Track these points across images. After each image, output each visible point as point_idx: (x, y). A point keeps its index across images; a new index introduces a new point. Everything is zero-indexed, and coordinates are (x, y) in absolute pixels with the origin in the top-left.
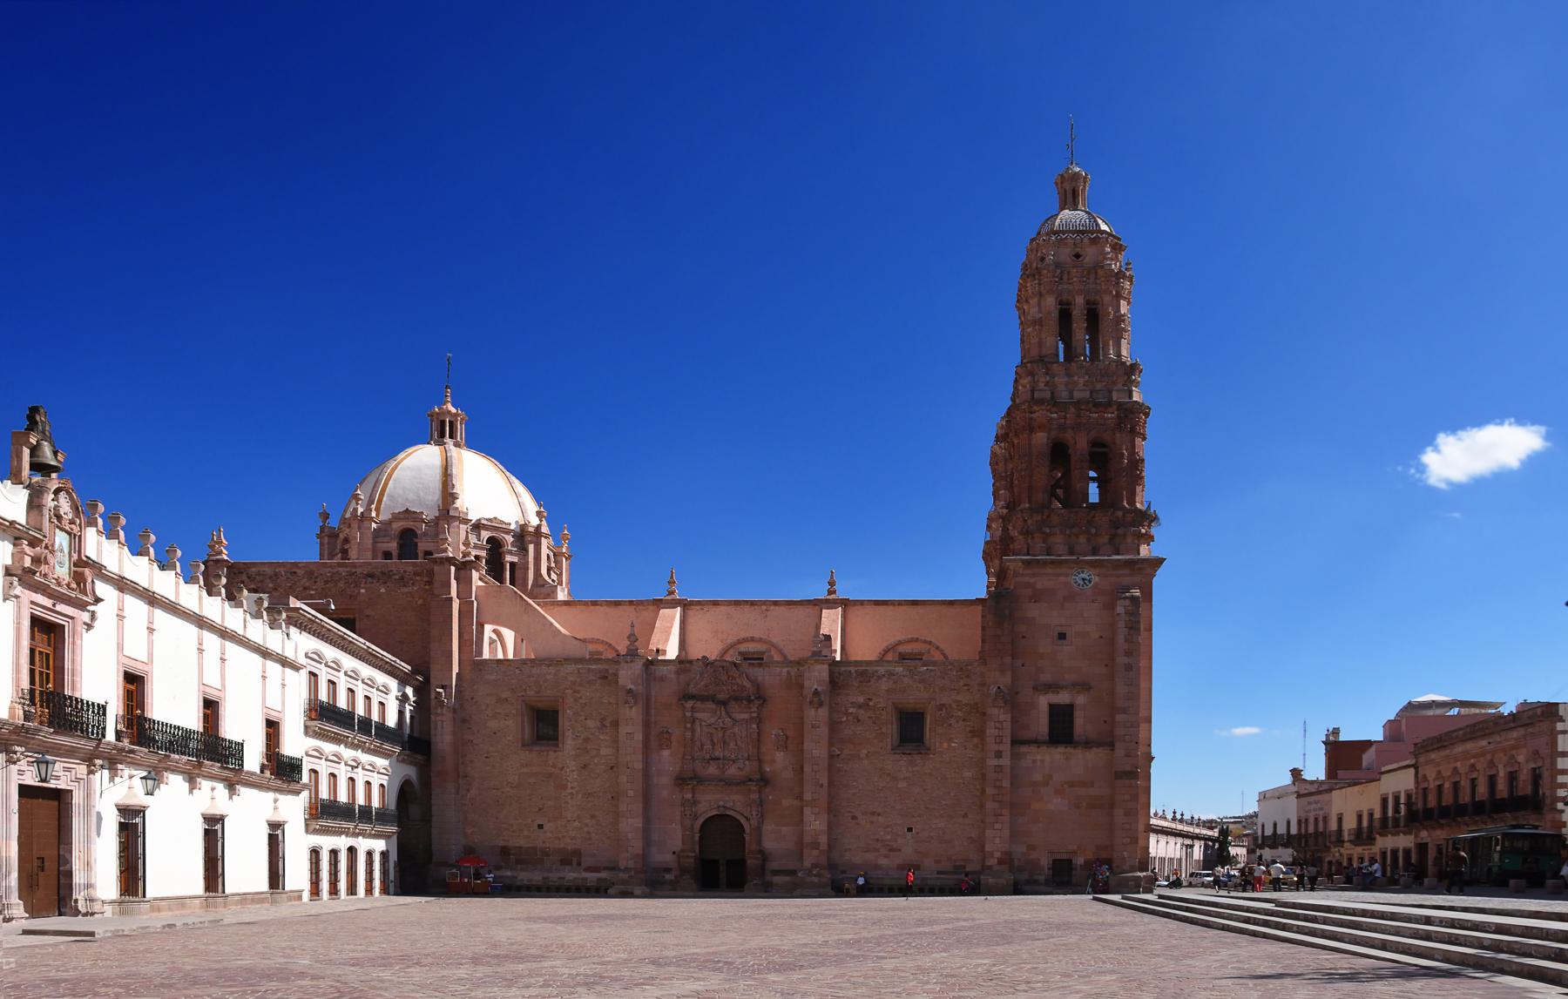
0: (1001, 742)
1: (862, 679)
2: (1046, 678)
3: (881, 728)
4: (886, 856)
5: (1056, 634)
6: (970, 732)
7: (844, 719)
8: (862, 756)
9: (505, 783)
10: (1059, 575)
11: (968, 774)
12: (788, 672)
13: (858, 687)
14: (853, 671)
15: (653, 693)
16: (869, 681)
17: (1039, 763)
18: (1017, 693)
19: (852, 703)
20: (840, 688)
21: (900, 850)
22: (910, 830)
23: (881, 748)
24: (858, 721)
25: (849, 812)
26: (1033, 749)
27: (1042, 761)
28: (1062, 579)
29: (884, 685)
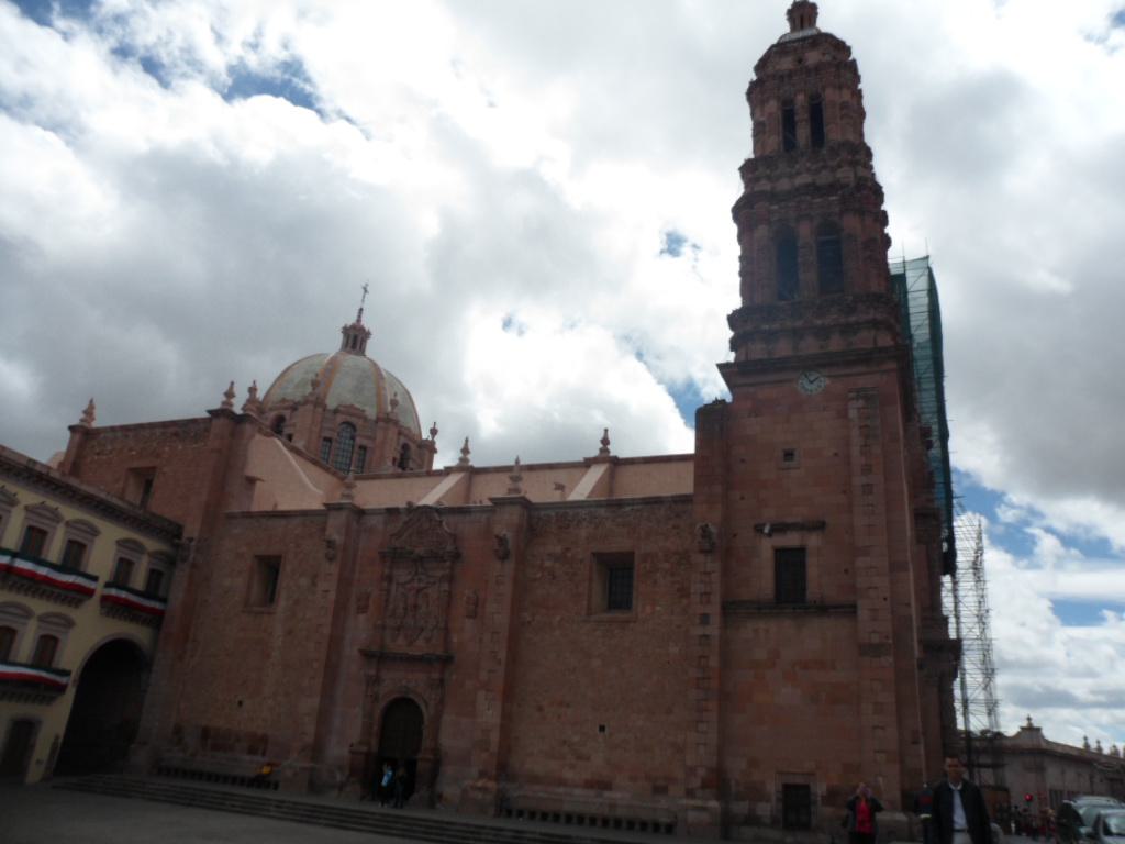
0: (708, 602)
2: (770, 514)
4: (572, 767)
5: (781, 454)
6: (678, 590)
7: (539, 575)
11: (674, 650)
14: (553, 514)
16: (568, 526)
18: (735, 536)
19: (549, 555)
21: (588, 759)
22: (602, 728)
24: (554, 578)
29: (583, 533)
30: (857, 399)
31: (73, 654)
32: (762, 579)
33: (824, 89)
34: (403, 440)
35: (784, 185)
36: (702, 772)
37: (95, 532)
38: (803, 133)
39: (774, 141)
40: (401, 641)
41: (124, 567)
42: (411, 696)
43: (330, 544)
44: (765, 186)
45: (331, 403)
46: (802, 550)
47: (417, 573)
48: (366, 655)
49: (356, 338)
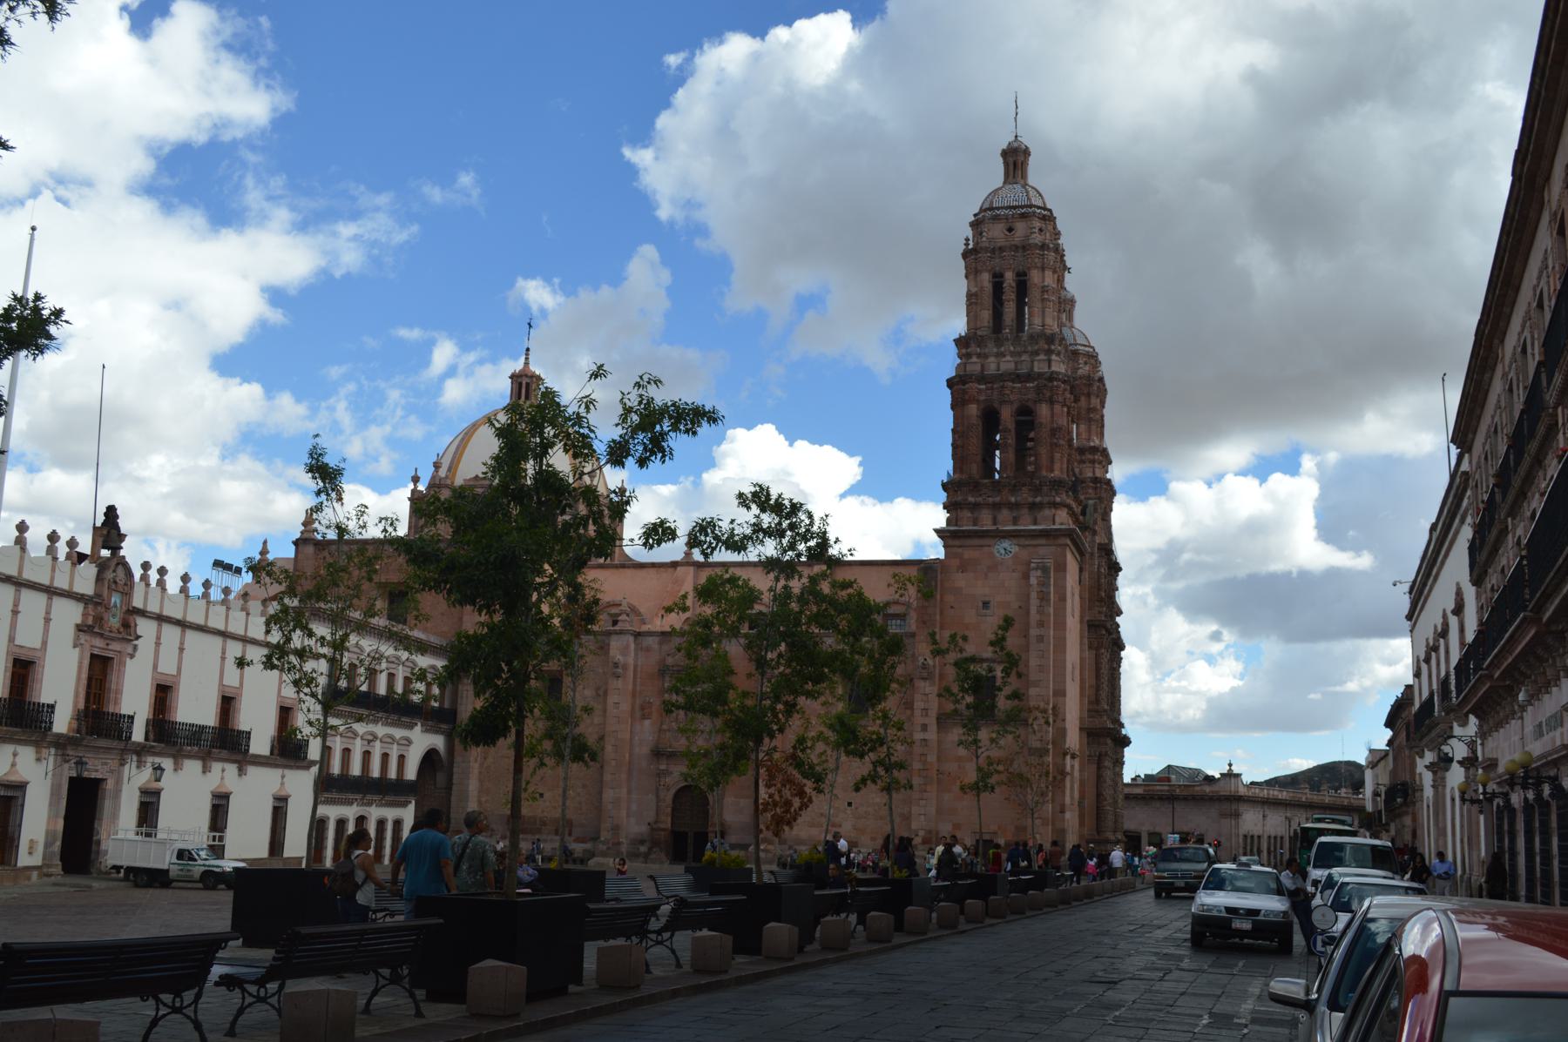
5: (981, 604)
10: (982, 546)
15: (639, 663)
21: (840, 826)
22: (850, 804)
30: (1037, 569)
31: (411, 773)
33: (1029, 268)
35: (992, 366)
36: (922, 833)
39: (986, 315)
40: (683, 741)
43: (616, 665)
44: (975, 367)
48: (658, 753)
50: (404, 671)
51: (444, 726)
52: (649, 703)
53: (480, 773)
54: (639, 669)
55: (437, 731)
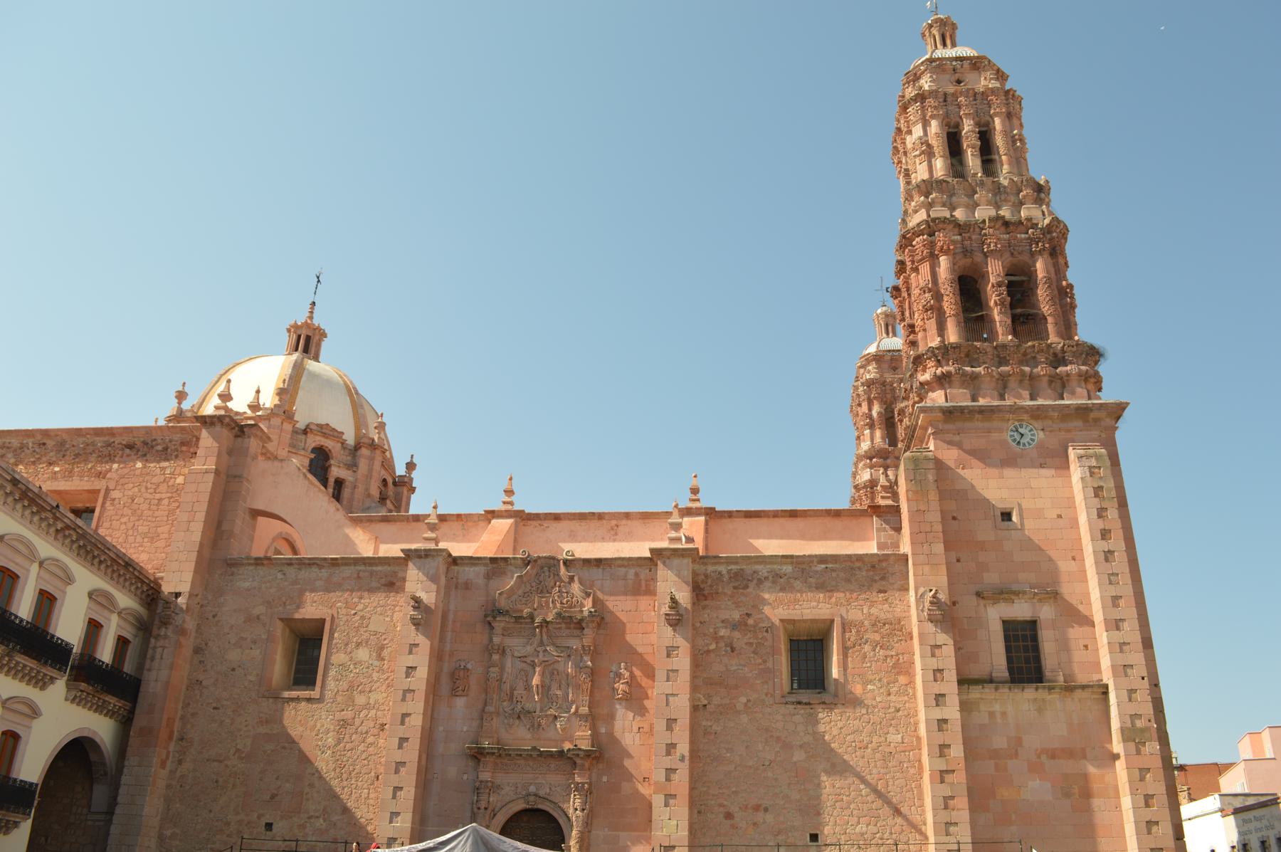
1: (736, 584)
2: (992, 578)
3: (765, 662)
7: (713, 647)
8: (740, 707)
9: (232, 752)
12: (637, 574)
13: (732, 596)
14: (724, 572)
15: (452, 607)
16: (746, 587)
17: (998, 716)
19: (723, 621)
20: (706, 598)
23: (766, 694)
24: (733, 650)
25: (721, 805)
26: (989, 689)
27: (1004, 714)
28: (995, 436)
32: (996, 657)
34: (384, 474)
37: (69, 579)
38: (972, 160)
41: (94, 628)
42: (540, 807)
45: (302, 420)
46: (1032, 625)
47: (541, 643)
49: (308, 338)
50: (39, 577)
51: (112, 700)
52: (466, 669)
53: (169, 787)
54: (451, 617)
55: (99, 709)
